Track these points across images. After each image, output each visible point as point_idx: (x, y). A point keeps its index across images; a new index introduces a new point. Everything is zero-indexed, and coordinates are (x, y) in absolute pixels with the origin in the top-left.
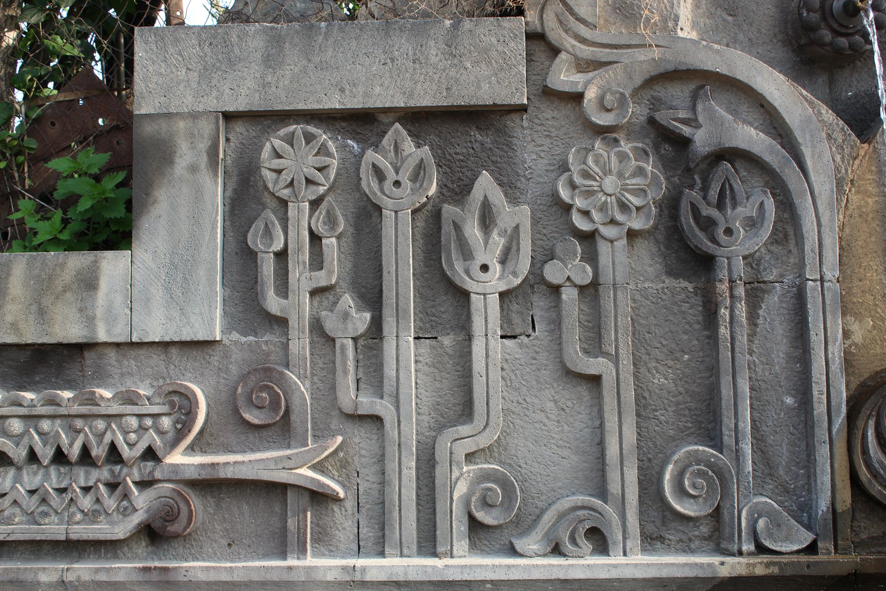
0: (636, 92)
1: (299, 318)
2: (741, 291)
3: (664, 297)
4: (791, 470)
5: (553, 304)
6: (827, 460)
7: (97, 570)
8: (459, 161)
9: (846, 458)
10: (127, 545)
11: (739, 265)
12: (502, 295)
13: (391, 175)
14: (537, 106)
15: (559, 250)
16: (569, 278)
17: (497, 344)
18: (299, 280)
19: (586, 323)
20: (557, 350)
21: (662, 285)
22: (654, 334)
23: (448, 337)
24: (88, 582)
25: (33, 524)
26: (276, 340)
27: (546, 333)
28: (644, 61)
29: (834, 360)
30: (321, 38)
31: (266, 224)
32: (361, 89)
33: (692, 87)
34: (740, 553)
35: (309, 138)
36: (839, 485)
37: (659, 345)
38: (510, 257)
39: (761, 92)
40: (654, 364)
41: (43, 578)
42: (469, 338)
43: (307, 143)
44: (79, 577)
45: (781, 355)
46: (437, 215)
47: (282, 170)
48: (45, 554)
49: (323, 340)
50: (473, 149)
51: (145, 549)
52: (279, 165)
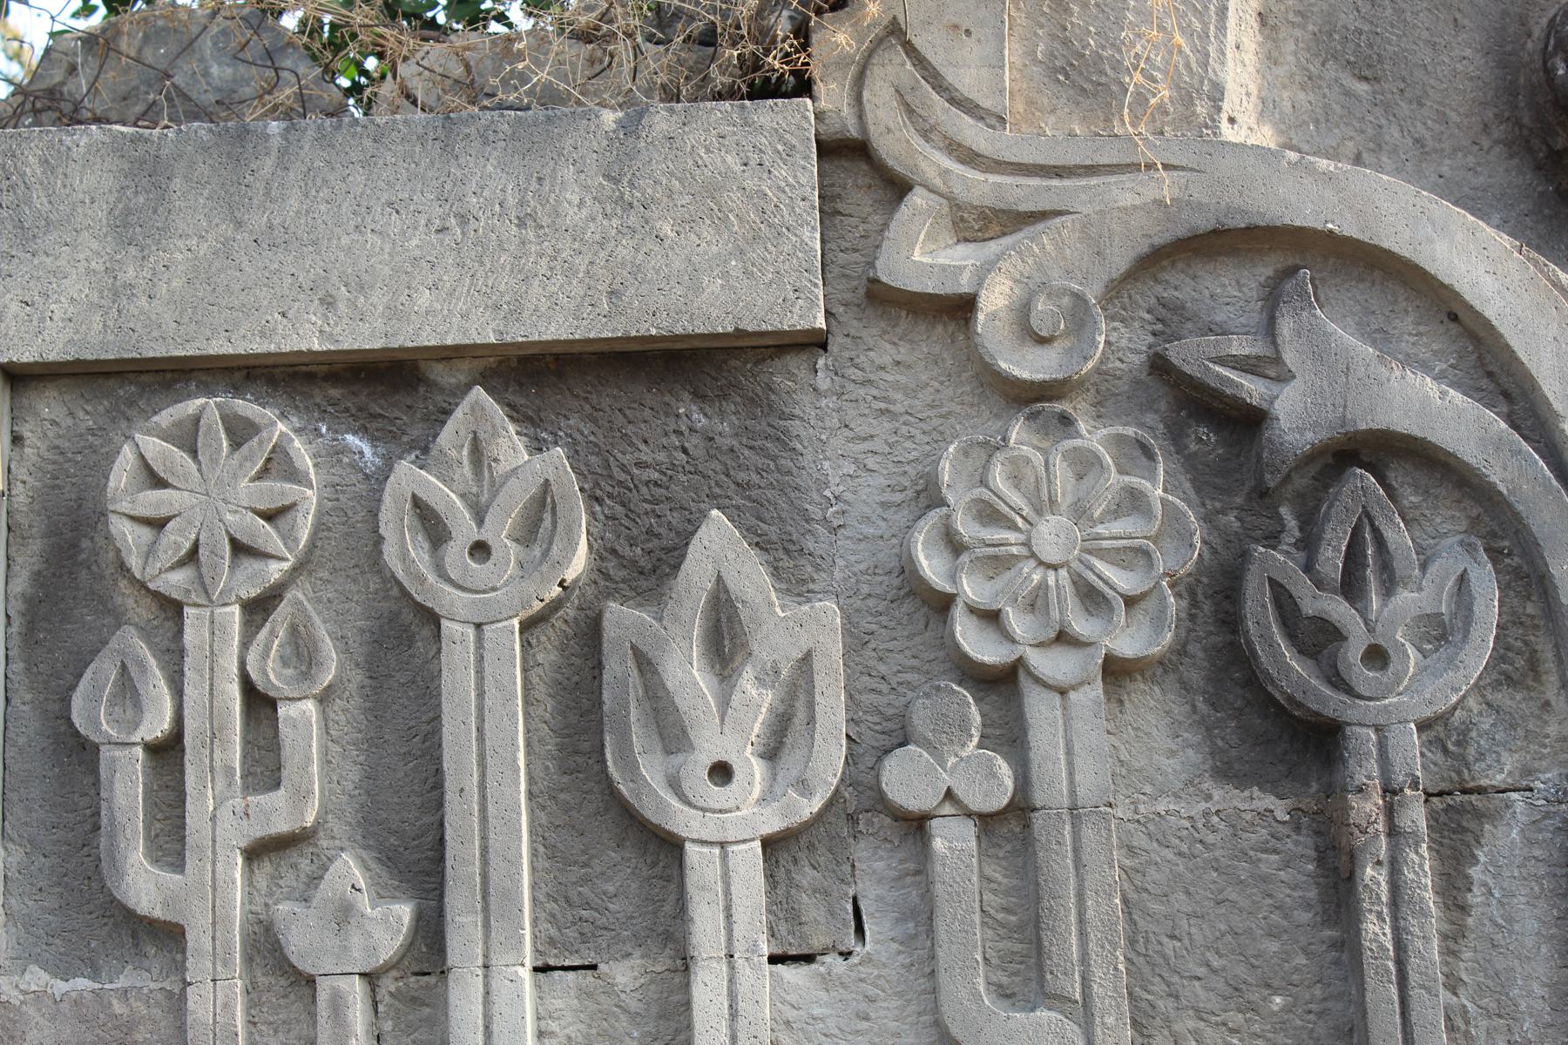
0: (1116, 289)
1: (214, 924)
2: (1416, 816)
3: (1210, 838)
5: (911, 866)
8: (647, 483)
11: (1410, 750)
12: (771, 845)
13: (464, 529)
14: (853, 332)
15: (921, 718)
16: (949, 795)
17: (758, 980)
18: (213, 819)
19: (1000, 916)
20: (924, 992)
21: (1203, 806)
22: (1186, 941)
23: (627, 963)
26: (153, 985)
27: (895, 946)
28: (1135, 207)
30: (269, 163)
31: (124, 666)
32: (379, 298)
33: (1265, 270)
35: (240, 432)
37: (1201, 971)
38: (788, 740)
39: (1447, 281)
40: (1191, 1024)
42: (685, 964)
43: (236, 444)
45: (1538, 990)
46: (590, 634)
47: (168, 519)
49: (283, 982)
50: (685, 451)
52: (159, 504)
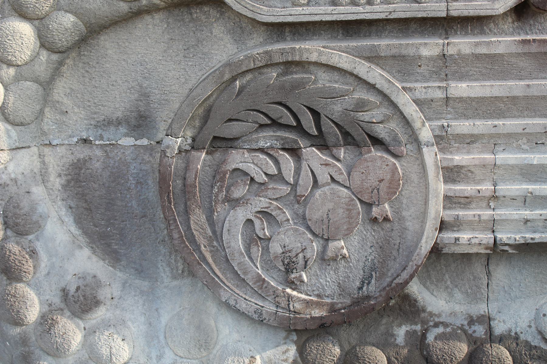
7: (477, 44)
10: (494, 22)
24: (468, 55)
25: (412, 3)
41: (425, 52)
44: (459, 50)
48: (413, 32)
51: (511, 25)
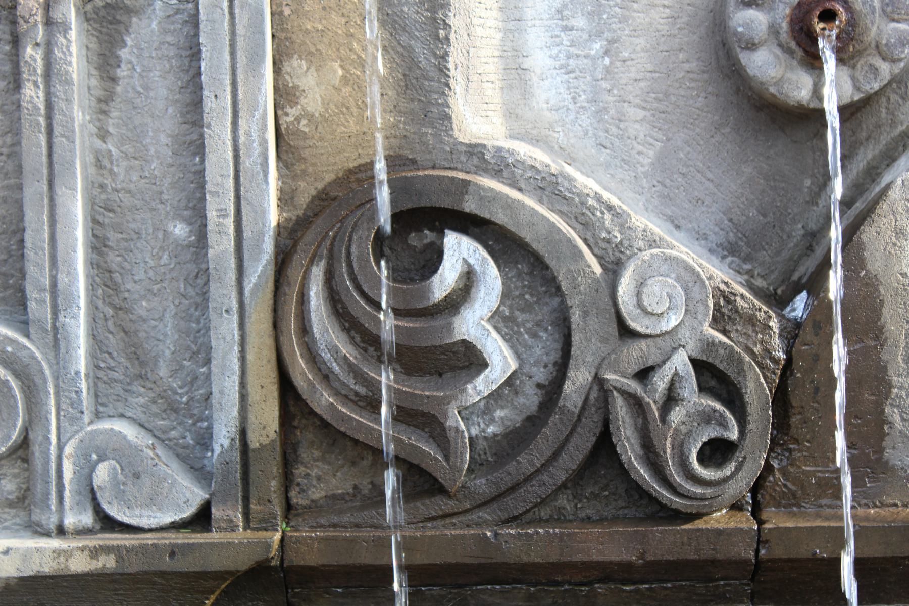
4: (182, 367)
6: (232, 348)
9: (269, 342)
29: (249, 148)
34: (61, 531)
36: (254, 394)
45: (164, 139)
